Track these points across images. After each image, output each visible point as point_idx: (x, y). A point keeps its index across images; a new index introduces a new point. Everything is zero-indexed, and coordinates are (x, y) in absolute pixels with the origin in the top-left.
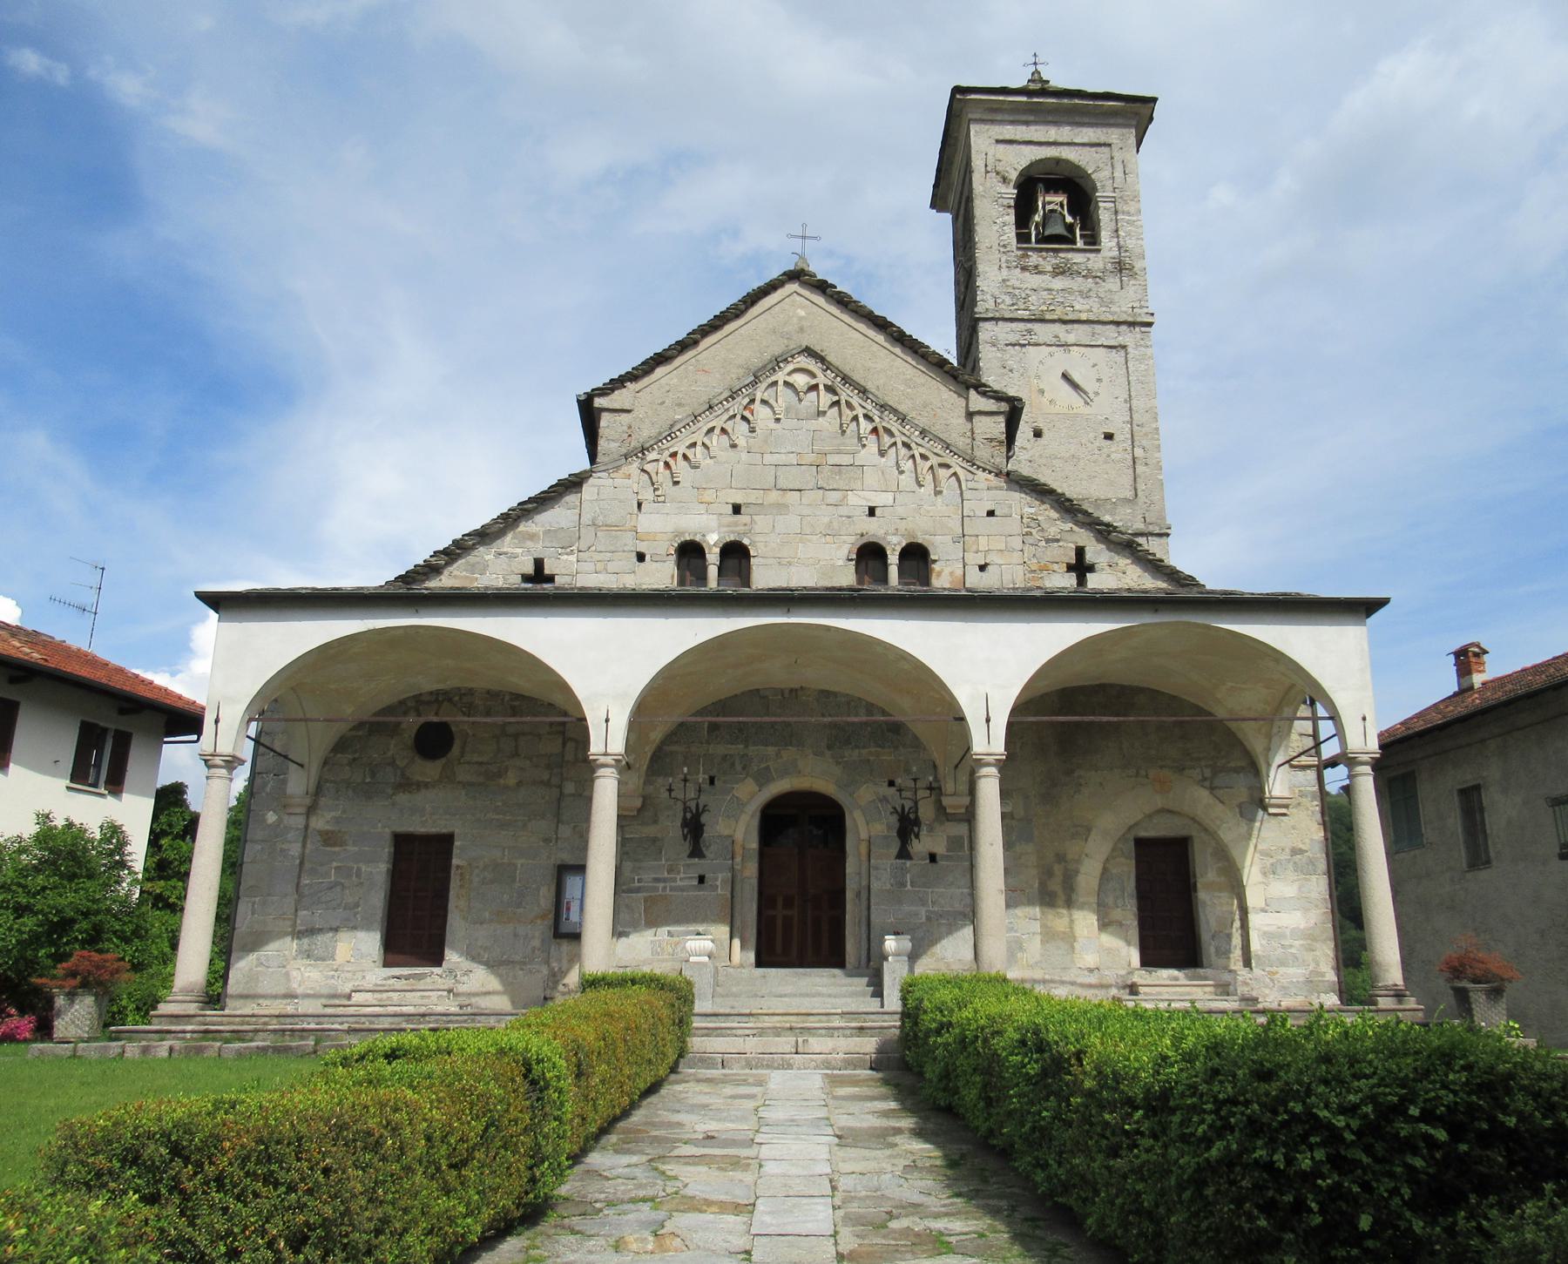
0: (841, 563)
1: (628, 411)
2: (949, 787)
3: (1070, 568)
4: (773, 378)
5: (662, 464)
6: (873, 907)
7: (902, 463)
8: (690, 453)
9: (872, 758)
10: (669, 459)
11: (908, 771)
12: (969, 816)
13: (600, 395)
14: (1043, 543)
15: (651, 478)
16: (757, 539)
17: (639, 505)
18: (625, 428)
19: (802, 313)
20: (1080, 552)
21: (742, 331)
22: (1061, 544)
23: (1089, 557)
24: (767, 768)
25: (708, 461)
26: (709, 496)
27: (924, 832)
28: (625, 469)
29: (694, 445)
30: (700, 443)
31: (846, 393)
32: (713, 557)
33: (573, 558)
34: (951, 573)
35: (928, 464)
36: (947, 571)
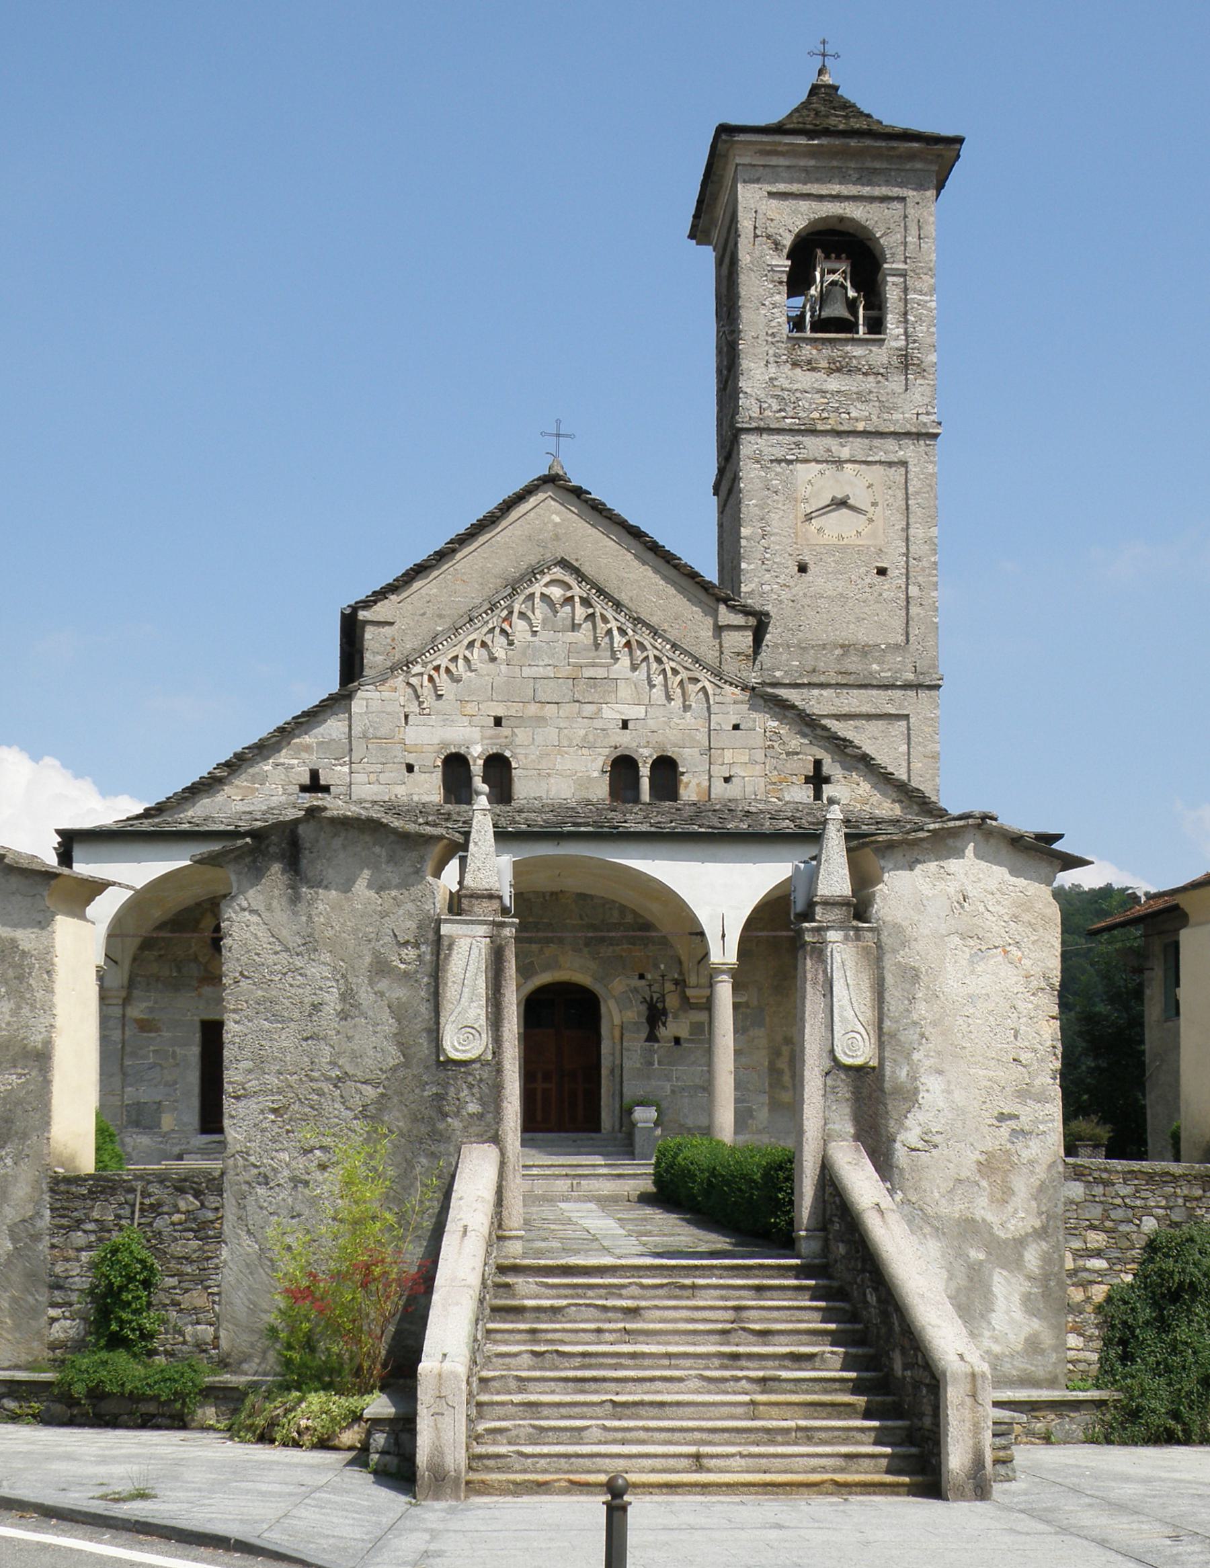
0: (596, 774)
1: (391, 624)
2: (692, 980)
3: (808, 780)
4: (530, 590)
5: (426, 677)
6: (625, 1083)
7: (653, 677)
8: (452, 667)
9: (624, 954)
10: (432, 672)
11: (657, 966)
12: (708, 1006)
13: (364, 608)
14: (784, 756)
15: (415, 691)
16: (518, 751)
17: (406, 717)
18: (389, 640)
19: (557, 519)
20: (818, 764)
21: (498, 538)
22: (800, 756)
23: (826, 769)
24: (532, 963)
25: (469, 674)
26: (471, 708)
27: (670, 1019)
28: (390, 683)
29: (455, 659)
30: (461, 656)
31: (600, 607)
32: (477, 768)
33: (346, 769)
34: (698, 785)
35: (679, 678)
36: (694, 782)
